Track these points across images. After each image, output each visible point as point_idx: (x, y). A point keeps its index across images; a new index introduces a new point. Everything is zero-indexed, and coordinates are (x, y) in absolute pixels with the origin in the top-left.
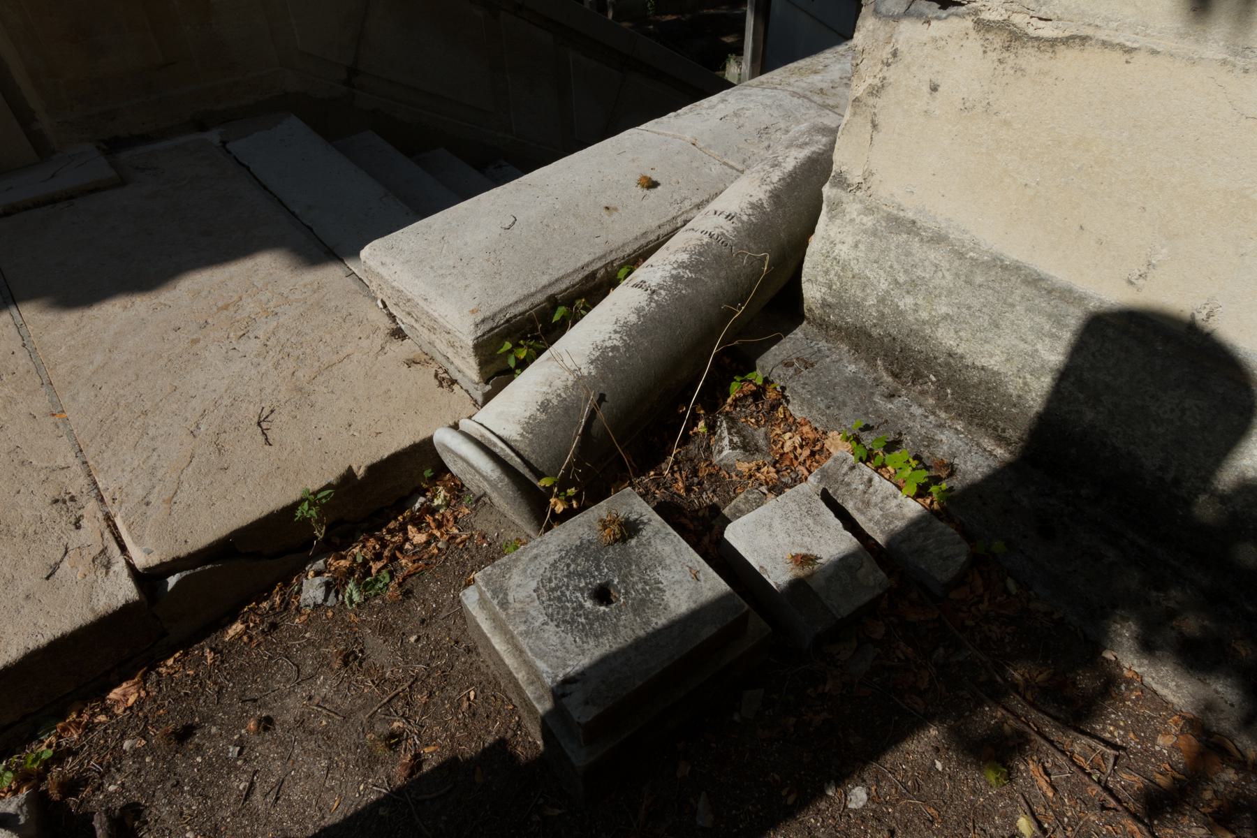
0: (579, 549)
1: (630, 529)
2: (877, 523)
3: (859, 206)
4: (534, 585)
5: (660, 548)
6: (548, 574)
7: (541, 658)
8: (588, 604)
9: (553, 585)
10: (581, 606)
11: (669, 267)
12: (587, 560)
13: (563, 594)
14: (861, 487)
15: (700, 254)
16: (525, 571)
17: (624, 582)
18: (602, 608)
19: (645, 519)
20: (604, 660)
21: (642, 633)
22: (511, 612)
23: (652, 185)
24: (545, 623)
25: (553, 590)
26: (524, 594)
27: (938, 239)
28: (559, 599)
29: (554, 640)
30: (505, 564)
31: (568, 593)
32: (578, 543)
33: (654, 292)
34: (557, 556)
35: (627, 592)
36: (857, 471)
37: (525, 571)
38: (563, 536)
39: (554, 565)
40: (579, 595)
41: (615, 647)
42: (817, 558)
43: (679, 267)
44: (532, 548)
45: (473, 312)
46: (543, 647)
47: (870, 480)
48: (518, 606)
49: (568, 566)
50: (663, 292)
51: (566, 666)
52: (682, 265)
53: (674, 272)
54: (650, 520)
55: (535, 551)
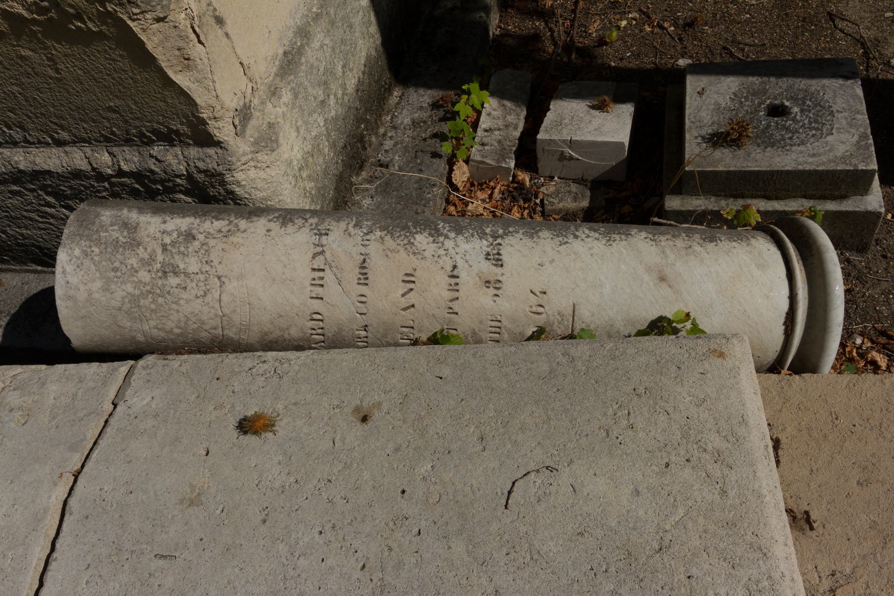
0: (772, 145)
1: (718, 140)
2: (518, 115)
3: (269, 105)
4: (829, 138)
5: (709, 117)
6: (812, 140)
7: (857, 96)
8: (796, 109)
9: (814, 132)
10: (802, 111)
11: (449, 244)
12: (772, 135)
13: (810, 123)
14: (497, 133)
15: (405, 228)
16: (830, 150)
17: (756, 111)
18: (787, 104)
19: (699, 140)
20: (812, 77)
21: (773, 79)
22: (862, 130)
23: (246, 426)
24: (838, 111)
25: (817, 129)
26: (842, 135)
27: (304, 33)
28: (816, 121)
29: (839, 101)
30: (845, 163)
31: (806, 122)
32: (769, 149)
33: (495, 237)
34: (794, 148)
35: (760, 104)
36: (485, 140)
37: (830, 150)
38: (778, 159)
39: (803, 143)
40: (798, 117)
41: (798, 80)
42: (590, 107)
43: (441, 235)
44: (811, 163)
45: (721, 355)
46: (851, 101)
47: (486, 131)
48: (853, 131)
49: (791, 138)
50: (488, 230)
51: (842, 85)
52: (435, 233)
53: (452, 235)
54: (696, 137)
55: (811, 160)
